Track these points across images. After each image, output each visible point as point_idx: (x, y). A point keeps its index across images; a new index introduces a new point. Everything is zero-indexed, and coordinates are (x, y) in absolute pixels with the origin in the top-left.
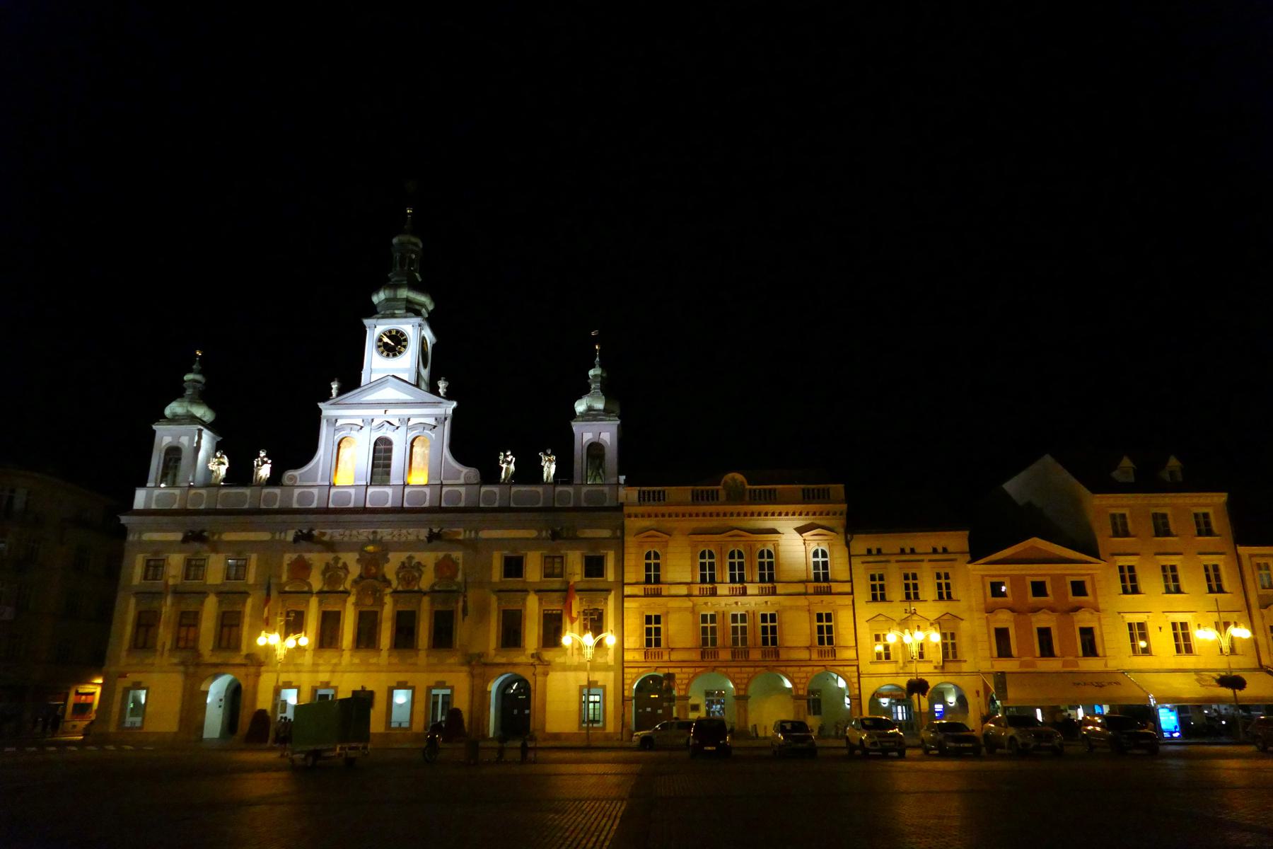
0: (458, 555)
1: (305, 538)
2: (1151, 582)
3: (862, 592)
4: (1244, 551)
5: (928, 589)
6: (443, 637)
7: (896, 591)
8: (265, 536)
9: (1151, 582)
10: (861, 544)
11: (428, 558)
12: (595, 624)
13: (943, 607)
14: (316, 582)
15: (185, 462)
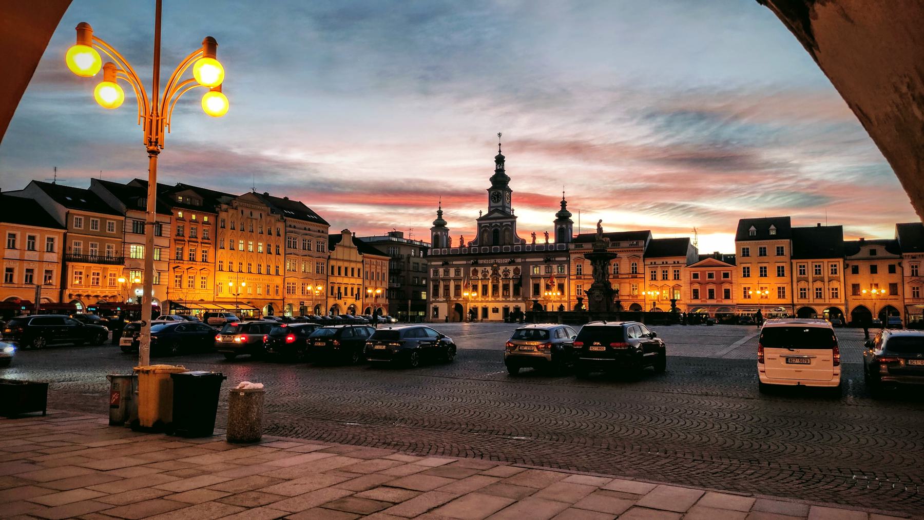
0: (520, 267)
1: (476, 264)
2: (755, 272)
3: (648, 276)
4: (794, 261)
5: (671, 276)
6: (517, 293)
7: (659, 276)
8: (465, 262)
9: (755, 272)
10: (648, 262)
11: (511, 268)
12: (561, 287)
13: (676, 282)
14: (480, 276)
15: (440, 239)
